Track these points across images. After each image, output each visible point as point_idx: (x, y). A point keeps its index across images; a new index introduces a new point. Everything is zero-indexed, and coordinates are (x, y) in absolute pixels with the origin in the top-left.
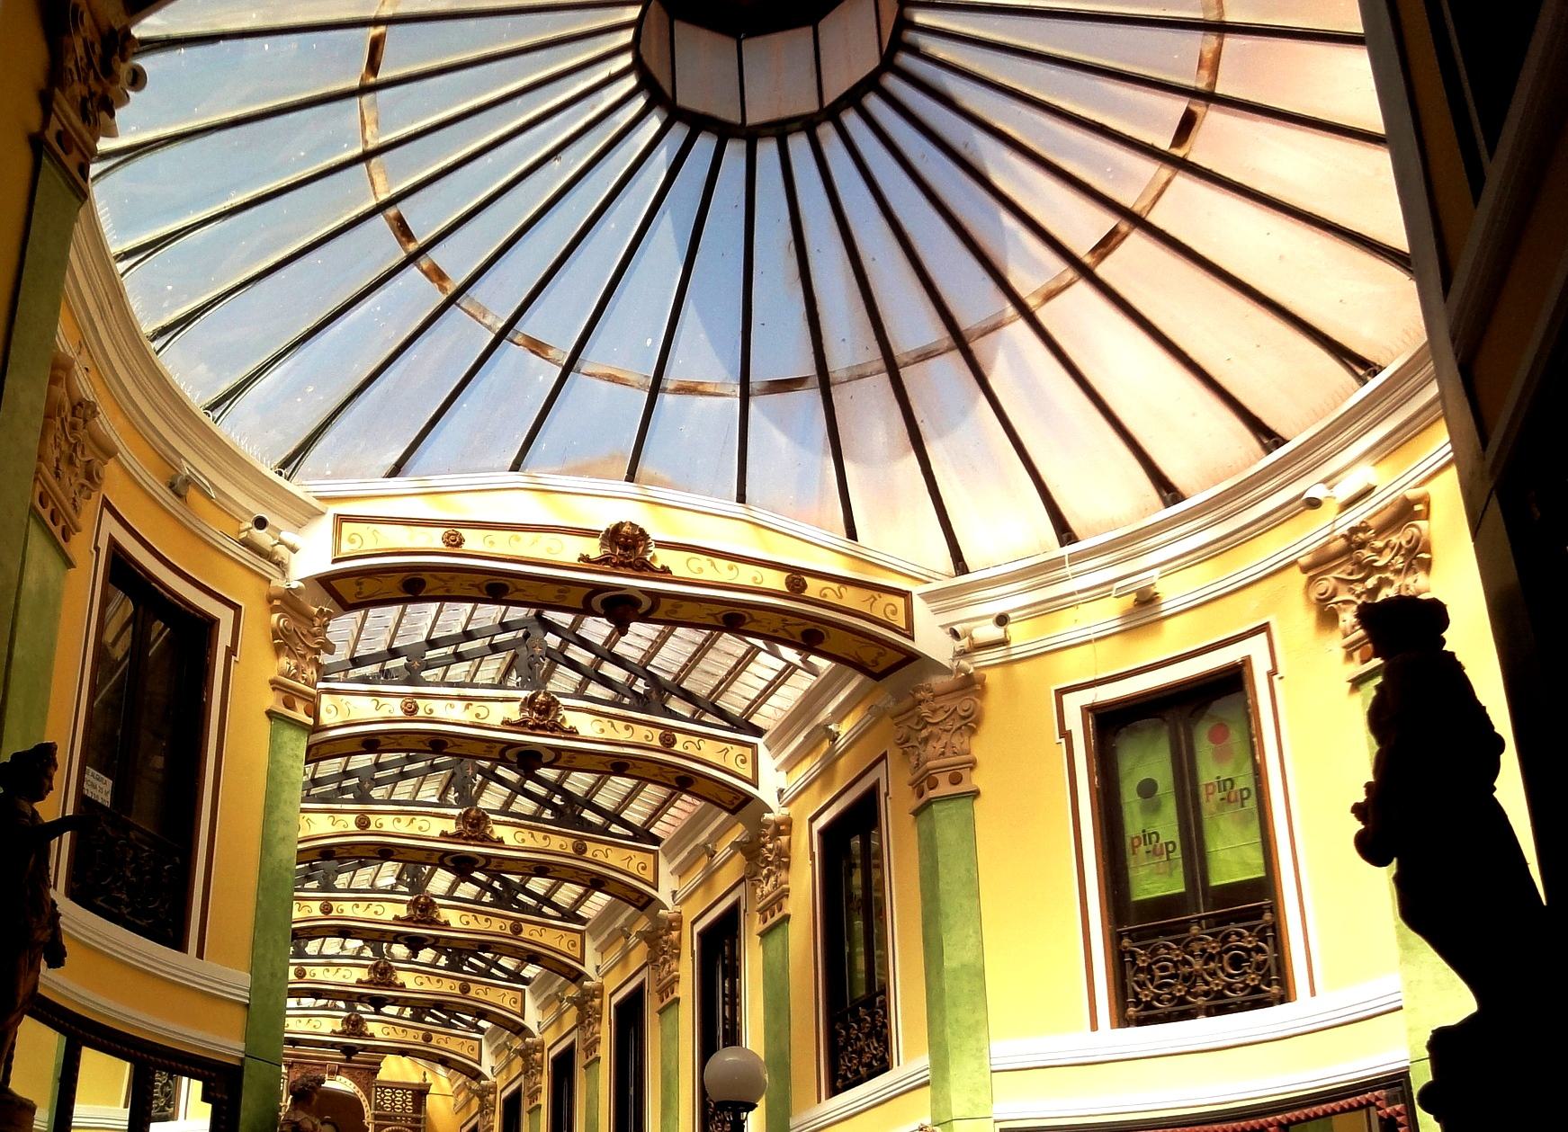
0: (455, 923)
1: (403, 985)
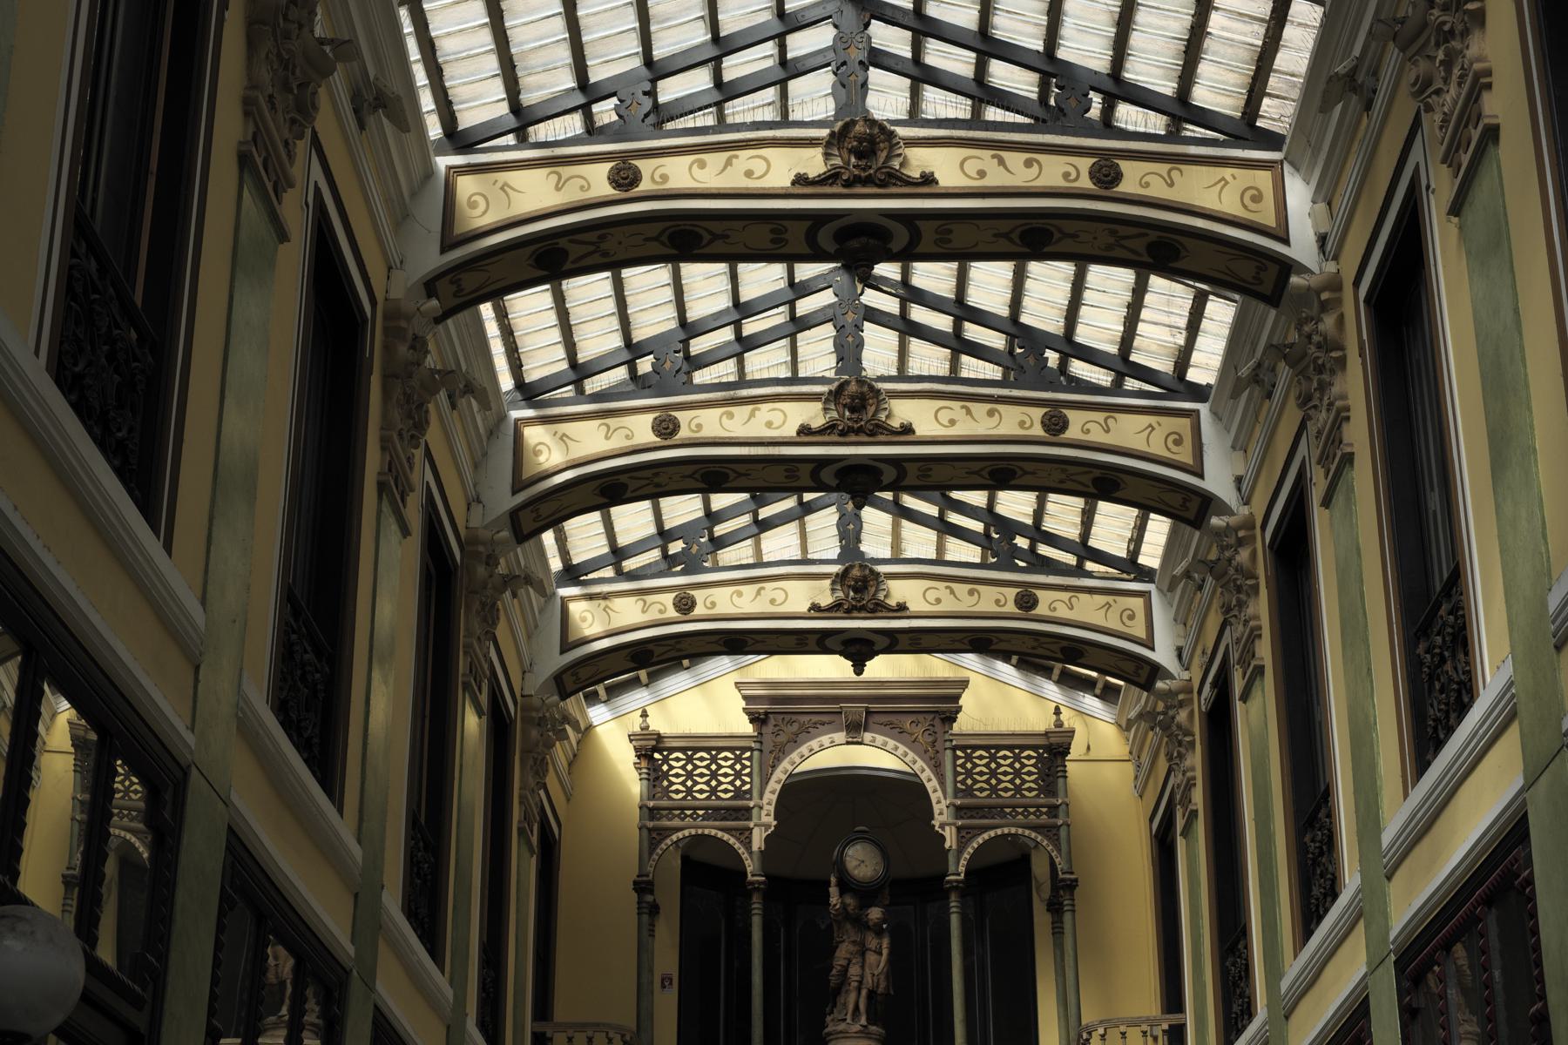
1: (907, 429)
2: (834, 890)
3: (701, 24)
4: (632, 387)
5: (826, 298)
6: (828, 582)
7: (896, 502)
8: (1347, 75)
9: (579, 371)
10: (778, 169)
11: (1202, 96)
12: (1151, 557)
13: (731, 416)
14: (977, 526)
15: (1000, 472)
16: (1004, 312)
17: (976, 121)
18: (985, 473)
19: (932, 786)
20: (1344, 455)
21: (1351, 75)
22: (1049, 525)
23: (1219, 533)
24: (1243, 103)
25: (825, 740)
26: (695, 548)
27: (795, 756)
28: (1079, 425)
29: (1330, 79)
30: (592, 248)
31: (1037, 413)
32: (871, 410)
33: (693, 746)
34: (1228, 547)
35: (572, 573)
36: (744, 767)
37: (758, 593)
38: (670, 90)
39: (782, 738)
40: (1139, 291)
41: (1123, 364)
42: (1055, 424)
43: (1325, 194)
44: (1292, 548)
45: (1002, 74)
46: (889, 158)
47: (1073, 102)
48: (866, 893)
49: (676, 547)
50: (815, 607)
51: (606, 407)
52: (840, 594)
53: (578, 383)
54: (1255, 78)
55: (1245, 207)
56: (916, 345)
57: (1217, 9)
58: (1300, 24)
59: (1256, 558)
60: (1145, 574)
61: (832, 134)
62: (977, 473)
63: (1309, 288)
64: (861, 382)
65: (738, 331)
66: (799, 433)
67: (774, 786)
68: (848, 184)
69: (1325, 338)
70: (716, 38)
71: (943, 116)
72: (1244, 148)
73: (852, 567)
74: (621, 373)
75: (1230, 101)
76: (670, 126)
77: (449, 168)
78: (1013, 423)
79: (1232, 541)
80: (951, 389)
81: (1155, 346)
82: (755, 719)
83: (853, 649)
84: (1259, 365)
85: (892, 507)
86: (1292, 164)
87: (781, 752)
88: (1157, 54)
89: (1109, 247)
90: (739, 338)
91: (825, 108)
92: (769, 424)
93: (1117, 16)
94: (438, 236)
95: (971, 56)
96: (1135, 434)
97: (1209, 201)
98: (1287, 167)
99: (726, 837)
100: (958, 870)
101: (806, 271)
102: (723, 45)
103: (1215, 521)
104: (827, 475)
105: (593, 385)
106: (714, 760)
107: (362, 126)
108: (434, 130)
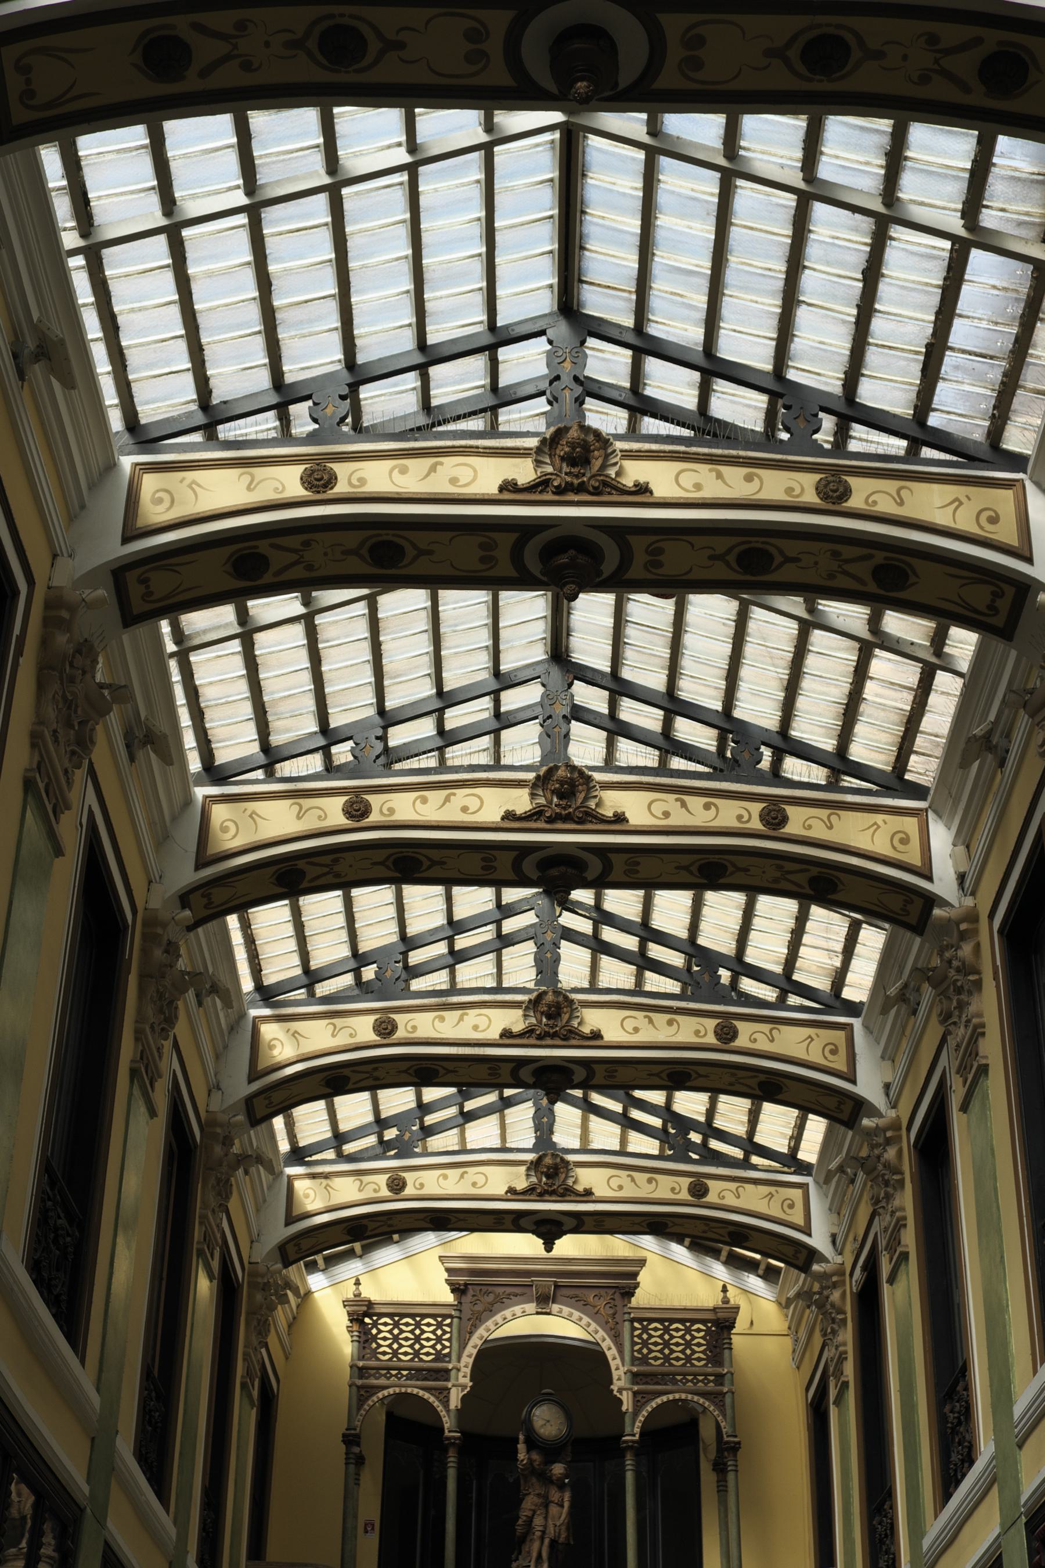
0: (637, 817)
1: (597, 1035)
2: (521, 1447)
3: (428, 680)
4: (356, 992)
5: (529, 919)
6: (523, 1169)
7: (586, 1099)
8: (983, 737)
9: (311, 977)
10: (488, 807)
11: (858, 752)
12: (809, 1153)
13: (442, 1019)
14: (656, 1122)
15: (677, 1075)
16: (684, 934)
17: (663, 769)
18: (664, 1075)
19: (612, 1354)
20: (980, 1066)
21: (988, 736)
22: (719, 1123)
23: (870, 1133)
24: (893, 759)
25: (518, 1309)
26: (407, 1136)
27: (490, 1324)
28: (747, 1035)
29: (969, 740)
30: (326, 870)
31: (711, 1024)
32: (565, 1017)
33: (400, 1312)
34: (878, 1145)
35: (298, 1155)
36: (445, 1332)
37: (462, 1176)
38: (398, 736)
39: (479, 1308)
40: (802, 918)
41: (786, 982)
42: (726, 1034)
43: (964, 838)
44: (934, 1147)
45: (686, 730)
46: (586, 799)
47: (746, 755)
48: (551, 1451)
49: (391, 1134)
50: (511, 1191)
51: (334, 1008)
52: (534, 1179)
53: (310, 987)
54: (904, 738)
55: (894, 848)
56: (606, 962)
57: (872, 678)
58: (943, 693)
59: (902, 1156)
60: (804, 1168)
61: (538, 777)
62: (658, 1075)
63: (949, 920)
64: (557, 992)
65: (451, 946)
66: (502, 1036)
67: (471, 1350)
68: (550, 820)
69: (964, 963)
70: (440, 693)
71: (634, 764)
72: (894, 797)
73: (545, 1155)
74: (348, 979)
75: (882, 757)
76: (397, 766)
77: (206, 797)
78: (690, 1032)
79: (881, 1140)
80: (635, 1000)
81: (815, 967)
82: (458, 1290)
83: (543, 1229)
84: (906, 986)
85: (581, 1103)
86: (935, 812)
87: (477, 1320)
88: (820, 715)
89: (776, 881)
90: (452, 951)
91: (532, 755)
92: (476, 1028)
93: (785, 683)
94: (194, 855)
95: (660, 713)
96: (796, 1044)
97: (863, 842)
98: (930, 814)
99: (426, 1395)
100: (633, 1431)
101: (512, 895)
102: (446, 699)
103: (866, 1122)
104: (525, 1074)
105: (323, 989)
106: (418, 1325)
107: (132, 759)
108: (195, 764)
